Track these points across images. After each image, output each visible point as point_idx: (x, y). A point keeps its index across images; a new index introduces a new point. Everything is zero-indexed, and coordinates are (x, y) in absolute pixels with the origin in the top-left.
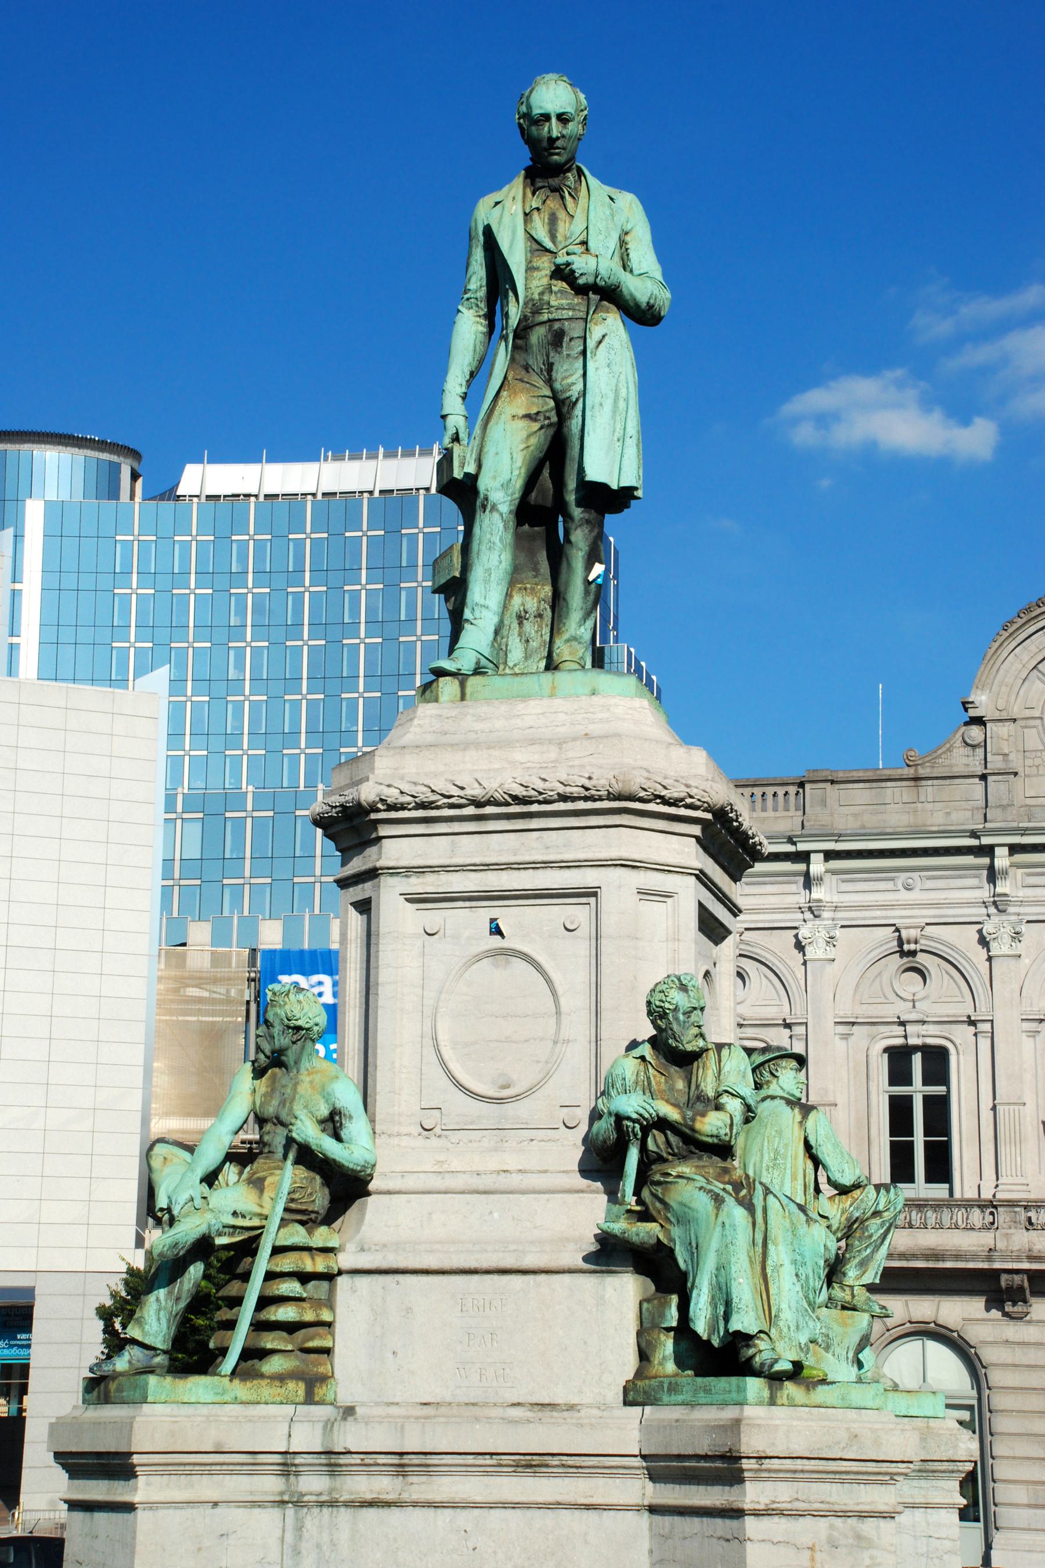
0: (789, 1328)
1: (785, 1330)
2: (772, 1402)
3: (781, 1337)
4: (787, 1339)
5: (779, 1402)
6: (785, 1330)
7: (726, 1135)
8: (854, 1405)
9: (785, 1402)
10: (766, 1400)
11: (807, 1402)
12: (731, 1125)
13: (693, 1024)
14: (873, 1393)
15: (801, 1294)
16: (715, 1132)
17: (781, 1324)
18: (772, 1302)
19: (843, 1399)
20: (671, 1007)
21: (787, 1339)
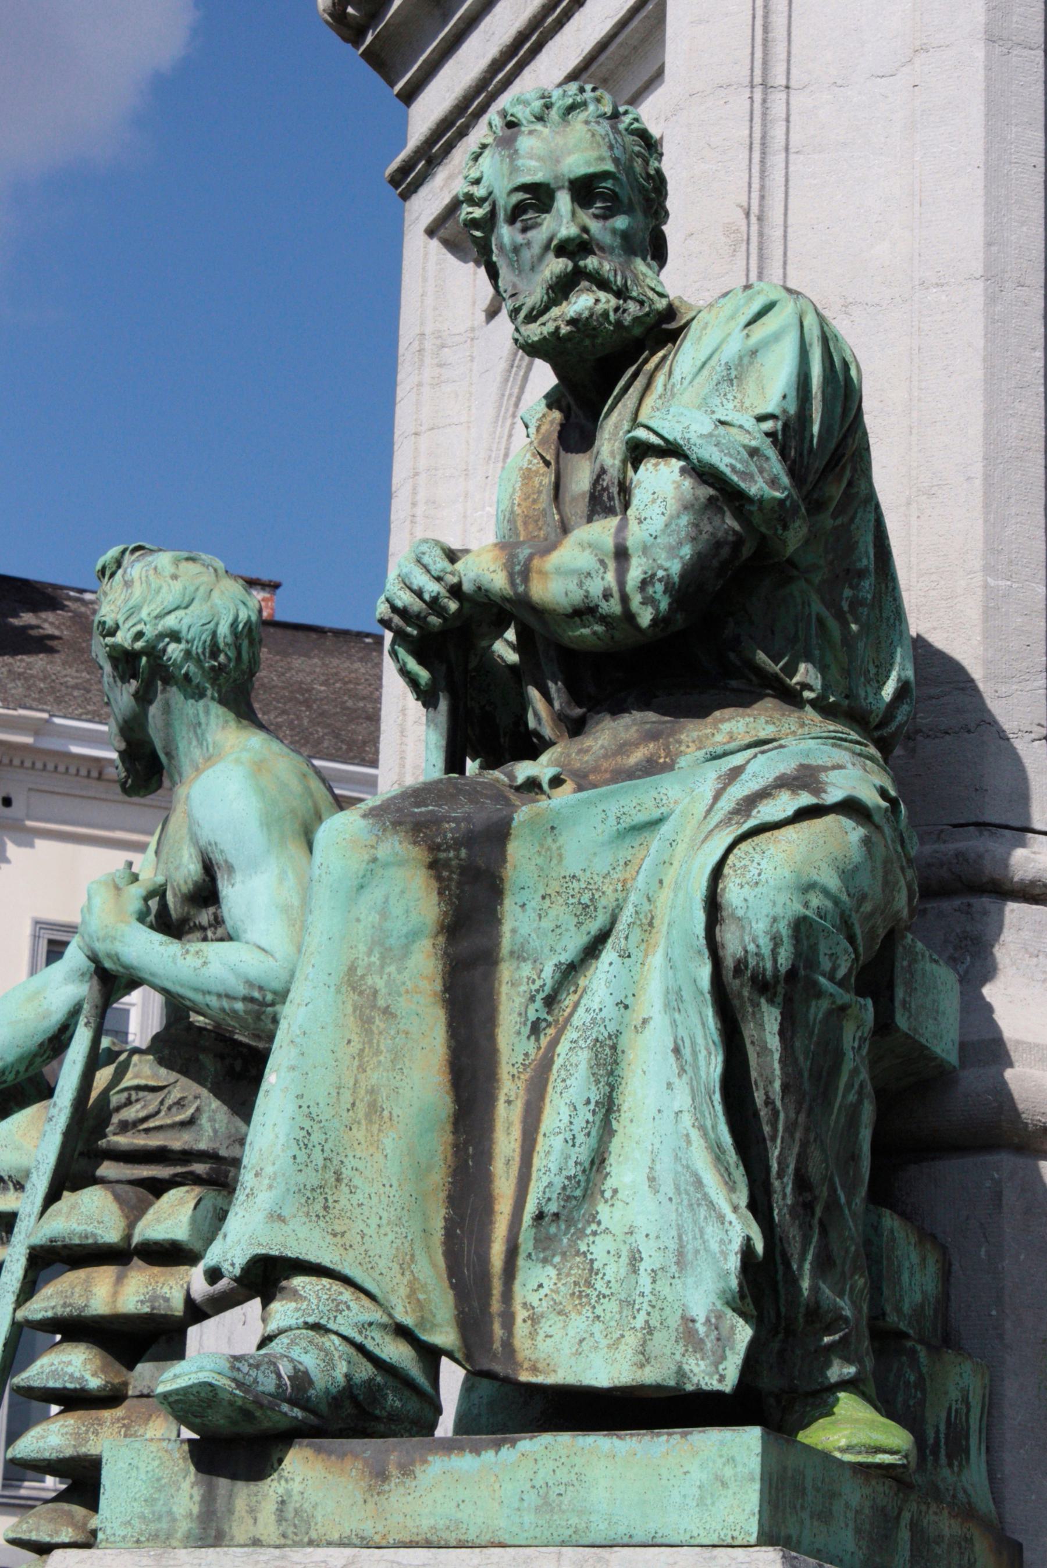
0: (635, 1259)
1: (614, 1270)
2: (211, 1532)
3: (584, 1291)
4: (611, 1307)
5: (240, 1530)
6: (614, 1270)
7: (607, 595)
8: (600, 1530)
9: (267, 1526)
10: (184, 1526)
11: (368, 1528)
12: (622, 554)
13: (547, 248)
14: (698, 1475)
15: (687, 1120)
16: (577, 596)
17: (600, 1249)
18: (537, 1162)
19: (546, 1506)
20: (478, 213)
21: (611, 1307)
